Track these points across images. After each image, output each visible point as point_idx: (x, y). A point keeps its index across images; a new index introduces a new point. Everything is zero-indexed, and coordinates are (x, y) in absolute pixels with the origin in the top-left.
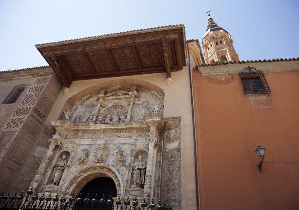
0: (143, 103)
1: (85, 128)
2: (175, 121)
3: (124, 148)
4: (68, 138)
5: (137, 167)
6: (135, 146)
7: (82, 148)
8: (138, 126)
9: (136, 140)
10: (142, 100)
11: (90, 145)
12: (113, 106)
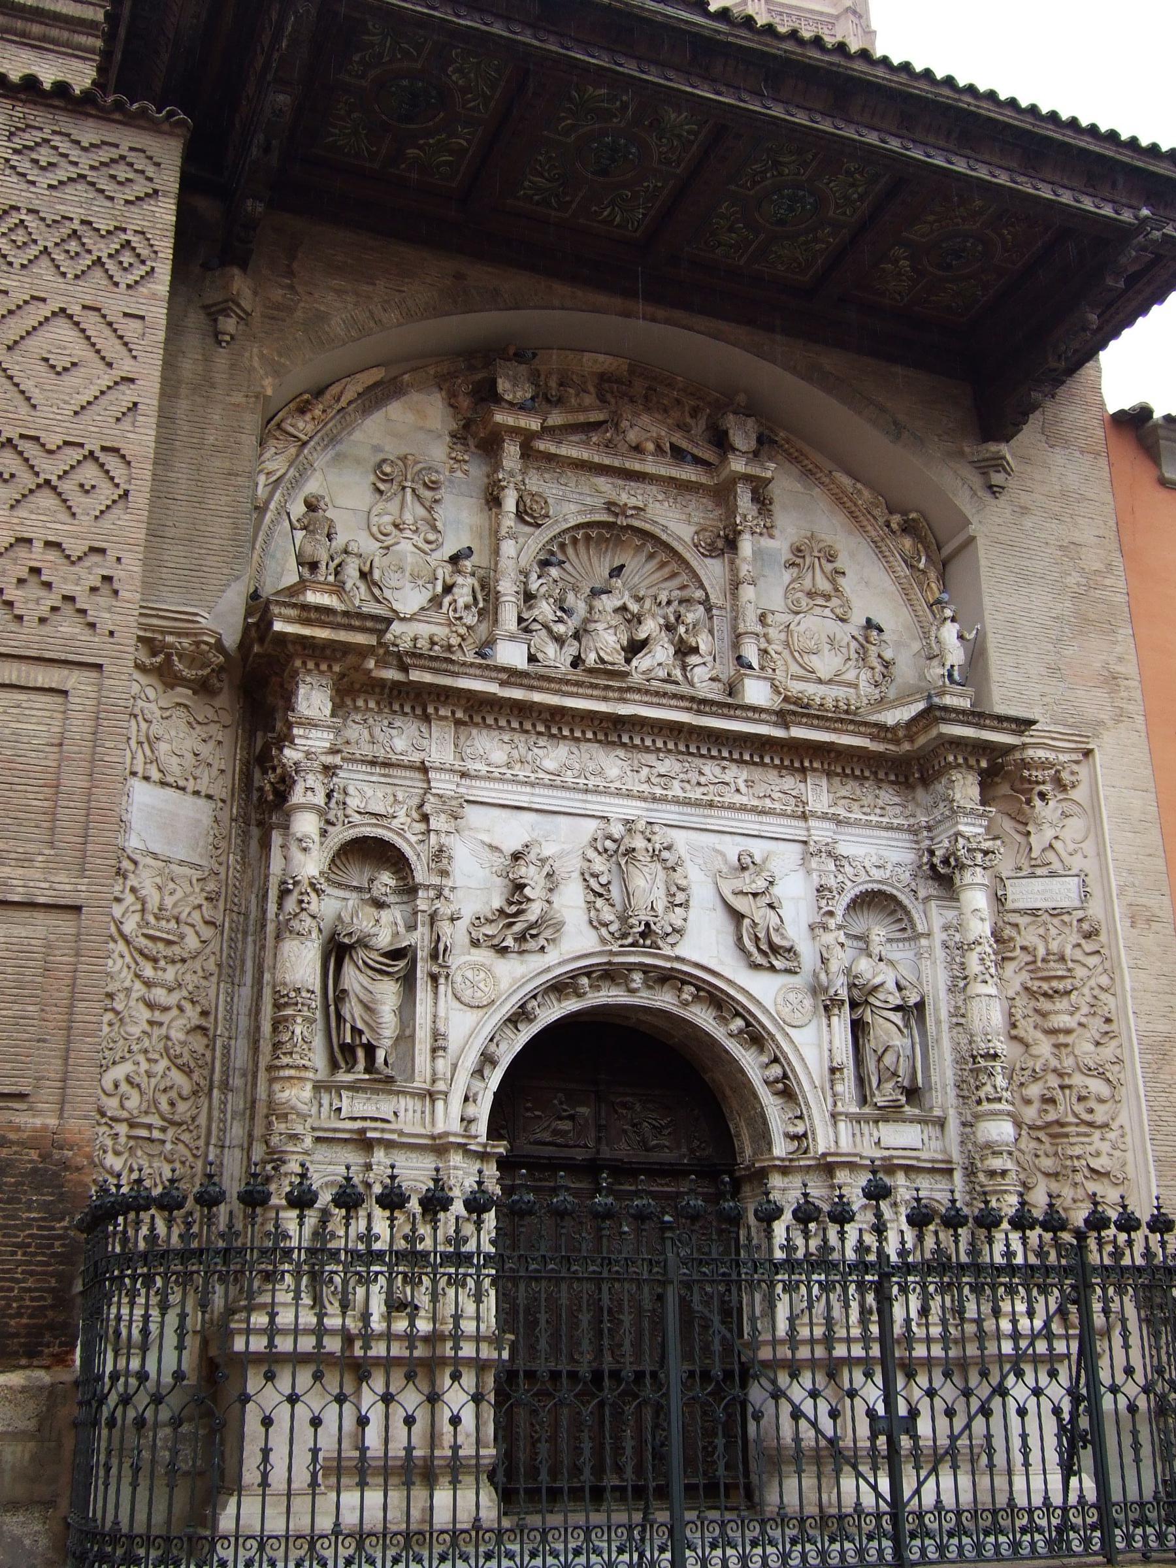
6: (839, 867)
12: (589, 525)
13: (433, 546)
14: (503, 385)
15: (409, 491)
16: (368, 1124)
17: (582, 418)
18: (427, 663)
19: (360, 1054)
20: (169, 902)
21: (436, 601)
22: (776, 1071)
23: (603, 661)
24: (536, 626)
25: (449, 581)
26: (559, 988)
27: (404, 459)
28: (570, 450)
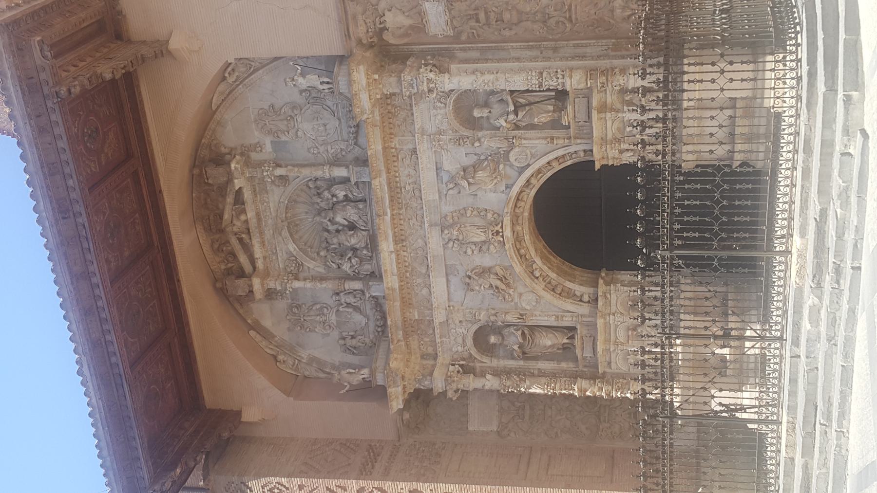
0: (270, 132)
1: (398, 304)
2: (354, 17)
3: (450, 165)
4: (430, 350)
5: (512, 117)
7: (458, 294)
8: (377, 132)
9: (423, 132)
10: (255, 136)
11: (447, 275)
12: (291, 235)
13: (329, 308)
15: (305, 318)
21: (357, 309)
22: (554, 164)
25: (345, 305)
27: (290, 320)
28: (258, 253)
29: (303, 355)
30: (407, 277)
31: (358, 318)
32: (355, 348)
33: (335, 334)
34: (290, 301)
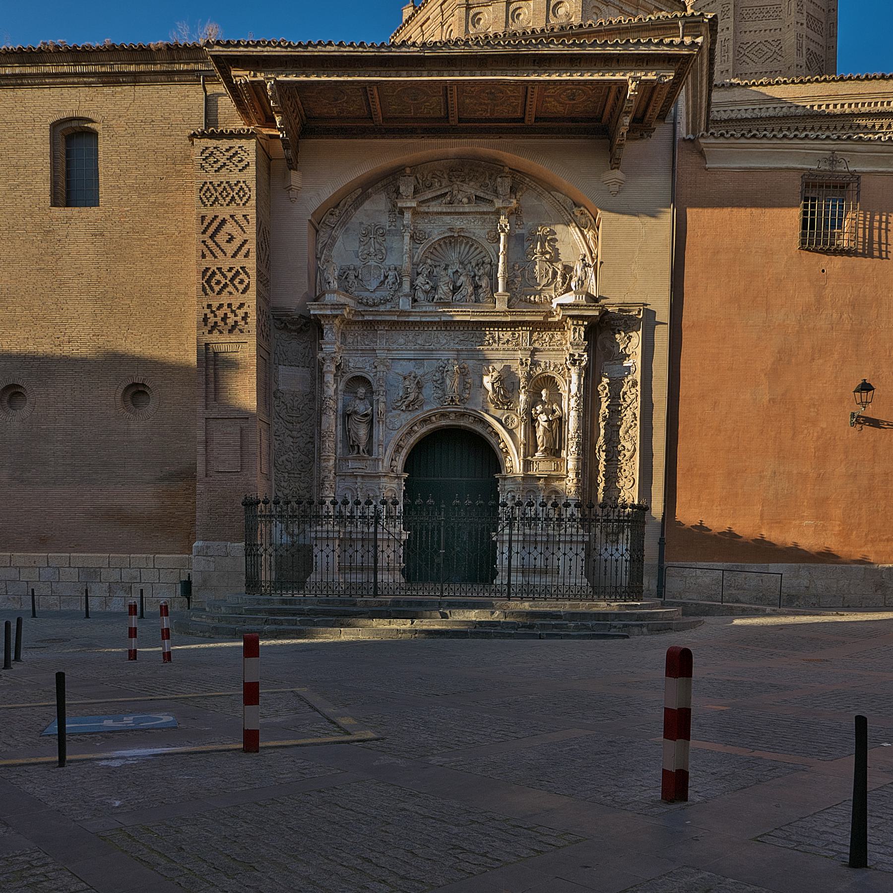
12: (445, 238)
14: (402, 189)
16: (356, 470)
17: (439, 193)
18: (370, 313)
19: (356, 448)
20: (296, 404)
21: (383, 283)
23: (441, 299)
24: (417, 288)
25: (386, 275)
26: (425, 421)
28: (434, 207)
29: (338, 232)
30: (414, 328)
31: (374, 284)
32: (346, 278)
33: (358, 263)
34: (388, 228)
